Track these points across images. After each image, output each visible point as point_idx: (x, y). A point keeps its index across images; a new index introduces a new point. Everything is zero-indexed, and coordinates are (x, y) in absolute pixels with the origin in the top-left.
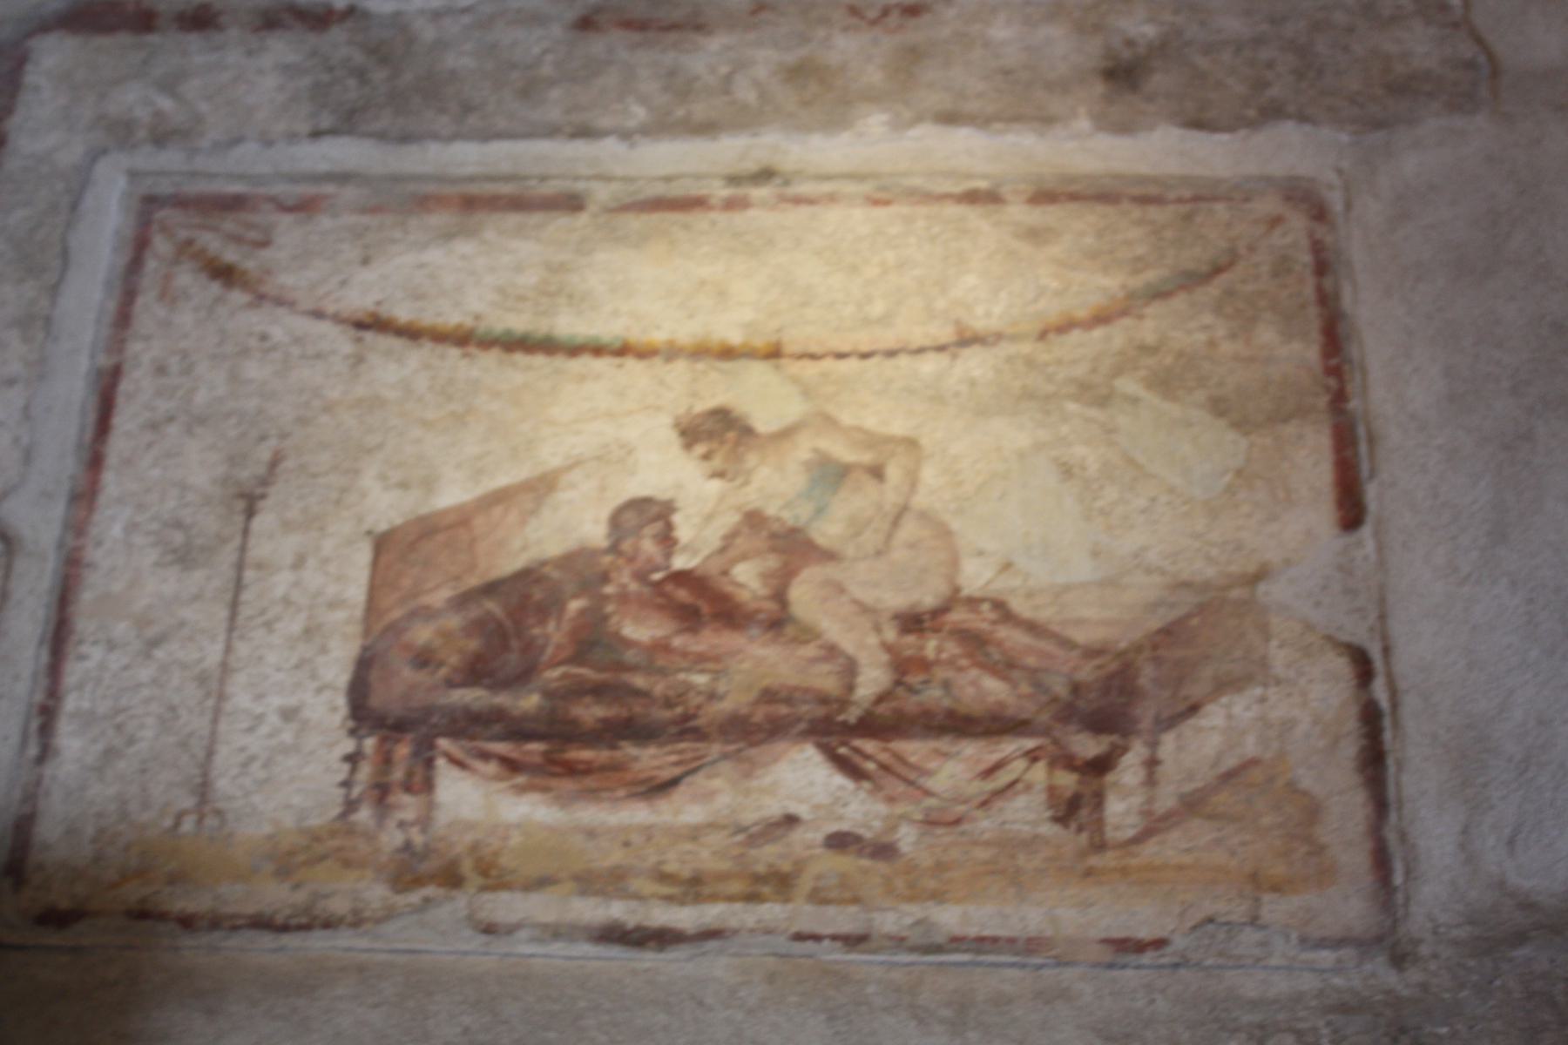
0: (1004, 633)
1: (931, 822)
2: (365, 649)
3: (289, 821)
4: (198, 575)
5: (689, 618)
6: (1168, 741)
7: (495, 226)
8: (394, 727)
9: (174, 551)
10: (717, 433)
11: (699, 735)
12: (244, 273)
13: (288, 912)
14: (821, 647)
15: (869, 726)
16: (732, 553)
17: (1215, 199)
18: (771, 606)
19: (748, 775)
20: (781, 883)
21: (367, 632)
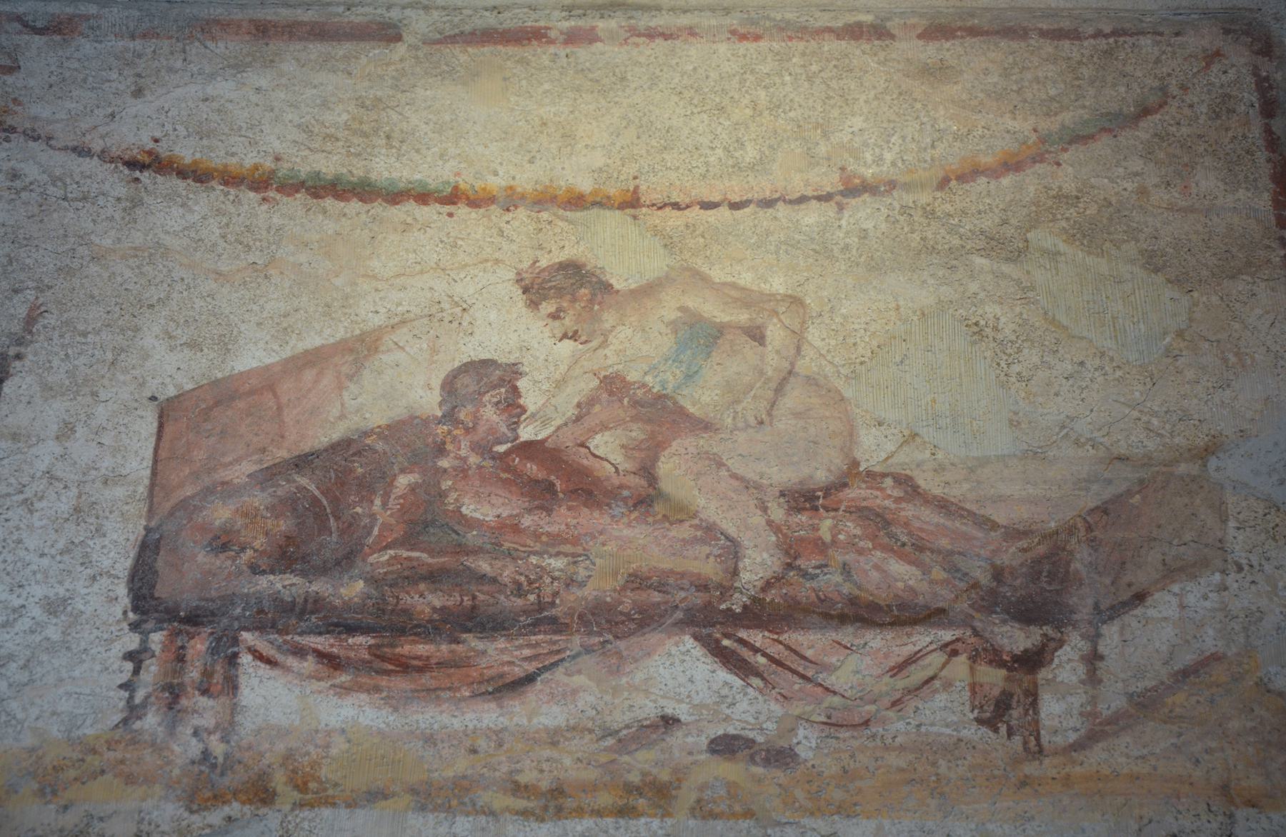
0: (909, 511)
2: (148, 530)
5: (542, 495)
6: (1111, 633)
10: (565, 289)
11: (556, 625)
14: (697, 527)
15: (756, 614)
16: (589, 422)
17: (1143, 33)
18: (637, 482)
19: (616, 671)
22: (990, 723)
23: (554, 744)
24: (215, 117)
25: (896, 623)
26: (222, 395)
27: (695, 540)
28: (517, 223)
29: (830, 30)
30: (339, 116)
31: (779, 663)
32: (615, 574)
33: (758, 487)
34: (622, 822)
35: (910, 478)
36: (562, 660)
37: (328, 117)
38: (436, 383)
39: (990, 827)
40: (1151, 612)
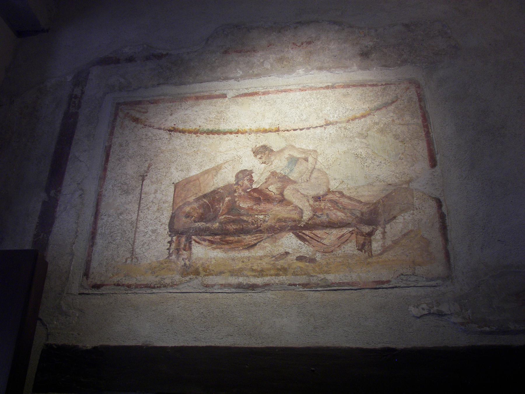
0: (342, 200)
3: (154, 259)
4: (131, 196)
5: (258, 201)
6: (388, 226)
7: (203, 104)
8: (181, 234)
9: (124, 191)
10: (263, 152)
11: (261, 232)
14: (293, 207)
16: (268, 183)
18: (278, 196)
19: (275, 242)
20: (284, 270)
23: (261, 260)
24: (187, 118)
25: (340, 227)
26: (188, 181)
27: (293, 210)
29: (322, 87)
31: (312, 238)
32: (274, 219)
33: (307, 196)
35: (342, 192)
37: (211, 116)
38: (234, 176)
39: (360, 274)
40: (397, 221)
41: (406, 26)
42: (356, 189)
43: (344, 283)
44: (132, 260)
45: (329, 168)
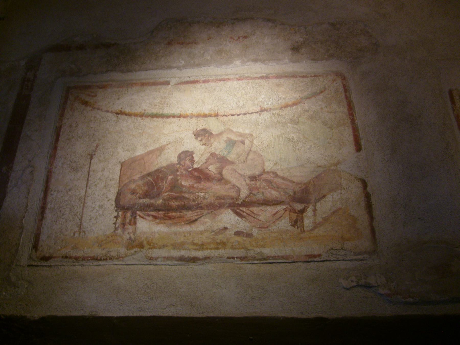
0: (276, 180)
1: (260, 228)
2: (119, 190)
5: (198, 180)
6: (318, 205)
8: (126, 209)
9: (73, 169)
10: (203, 135)
11: (201, 208)
12: (90, 103)
13: (101, 256)
14: (231, 185)
17: (320, 76)
19: (214, 218)
20: (223, 244)
21: (119, 186)
22: (293, 226)
23: (201, 234)
25: (274, 204)
26: (133, 160)
28: (193, 121)
29: (257, 78)
30: (157, 101)
31: (249, 215)
32: (214, 196)
33: (244, 176)
34: (216, 251)
36: (203, 216)
38: (176, 156)
39: (294, 248)
40: (327, 200)
41: (332, 25)
42: (289, 170)
43: (278, 256)
44: (80, 234)
45: (264, 151)
